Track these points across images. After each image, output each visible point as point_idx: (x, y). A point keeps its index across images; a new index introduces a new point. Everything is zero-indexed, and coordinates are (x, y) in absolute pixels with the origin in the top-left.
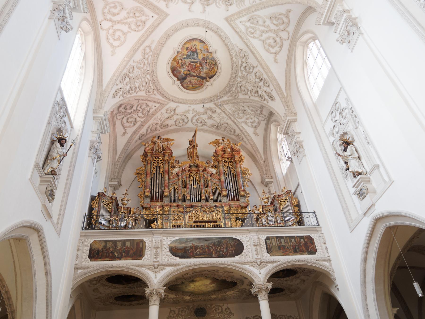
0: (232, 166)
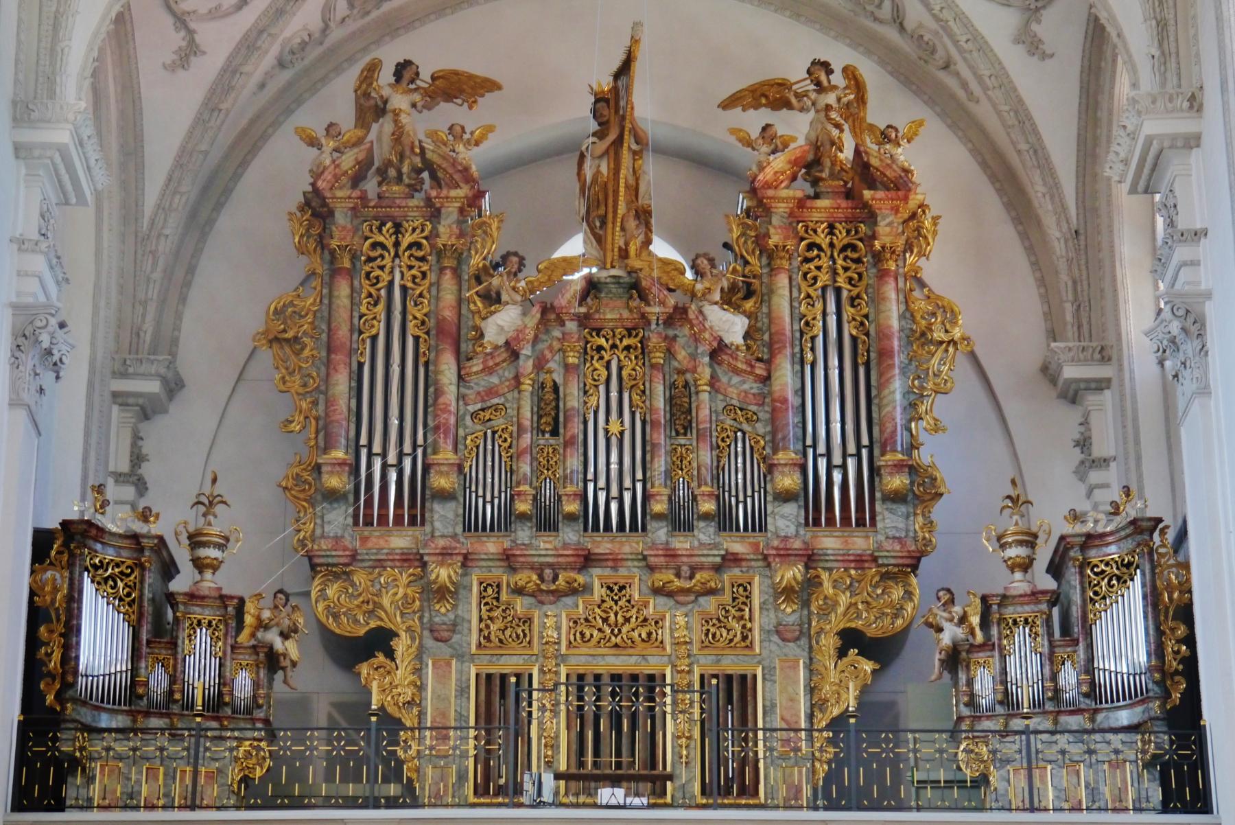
0: (850, 280)
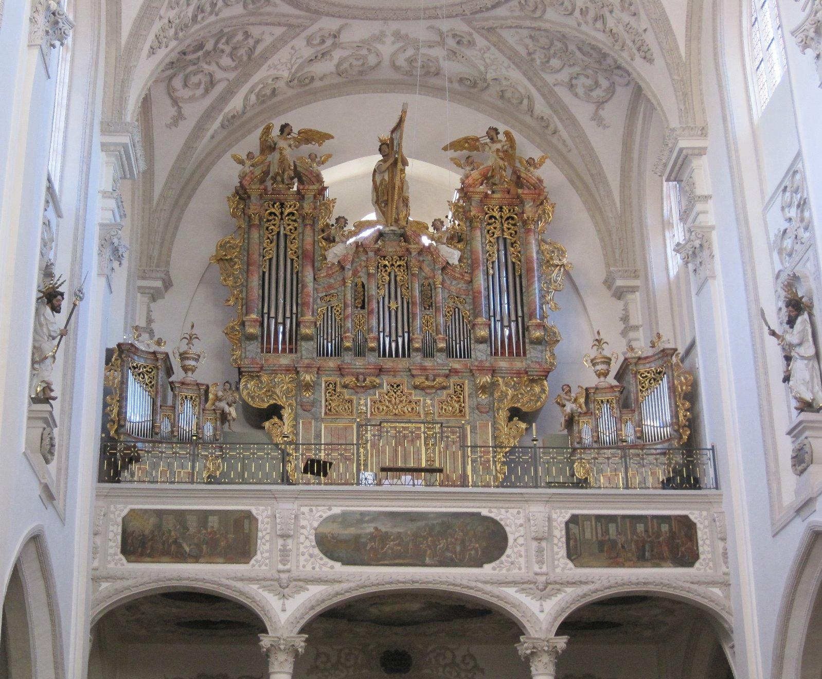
0: (511, 234)
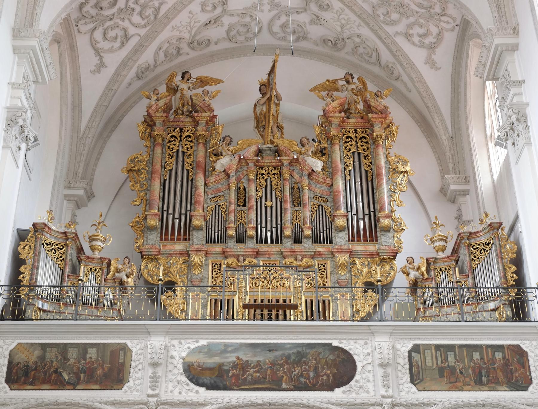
0: (364, 150)
